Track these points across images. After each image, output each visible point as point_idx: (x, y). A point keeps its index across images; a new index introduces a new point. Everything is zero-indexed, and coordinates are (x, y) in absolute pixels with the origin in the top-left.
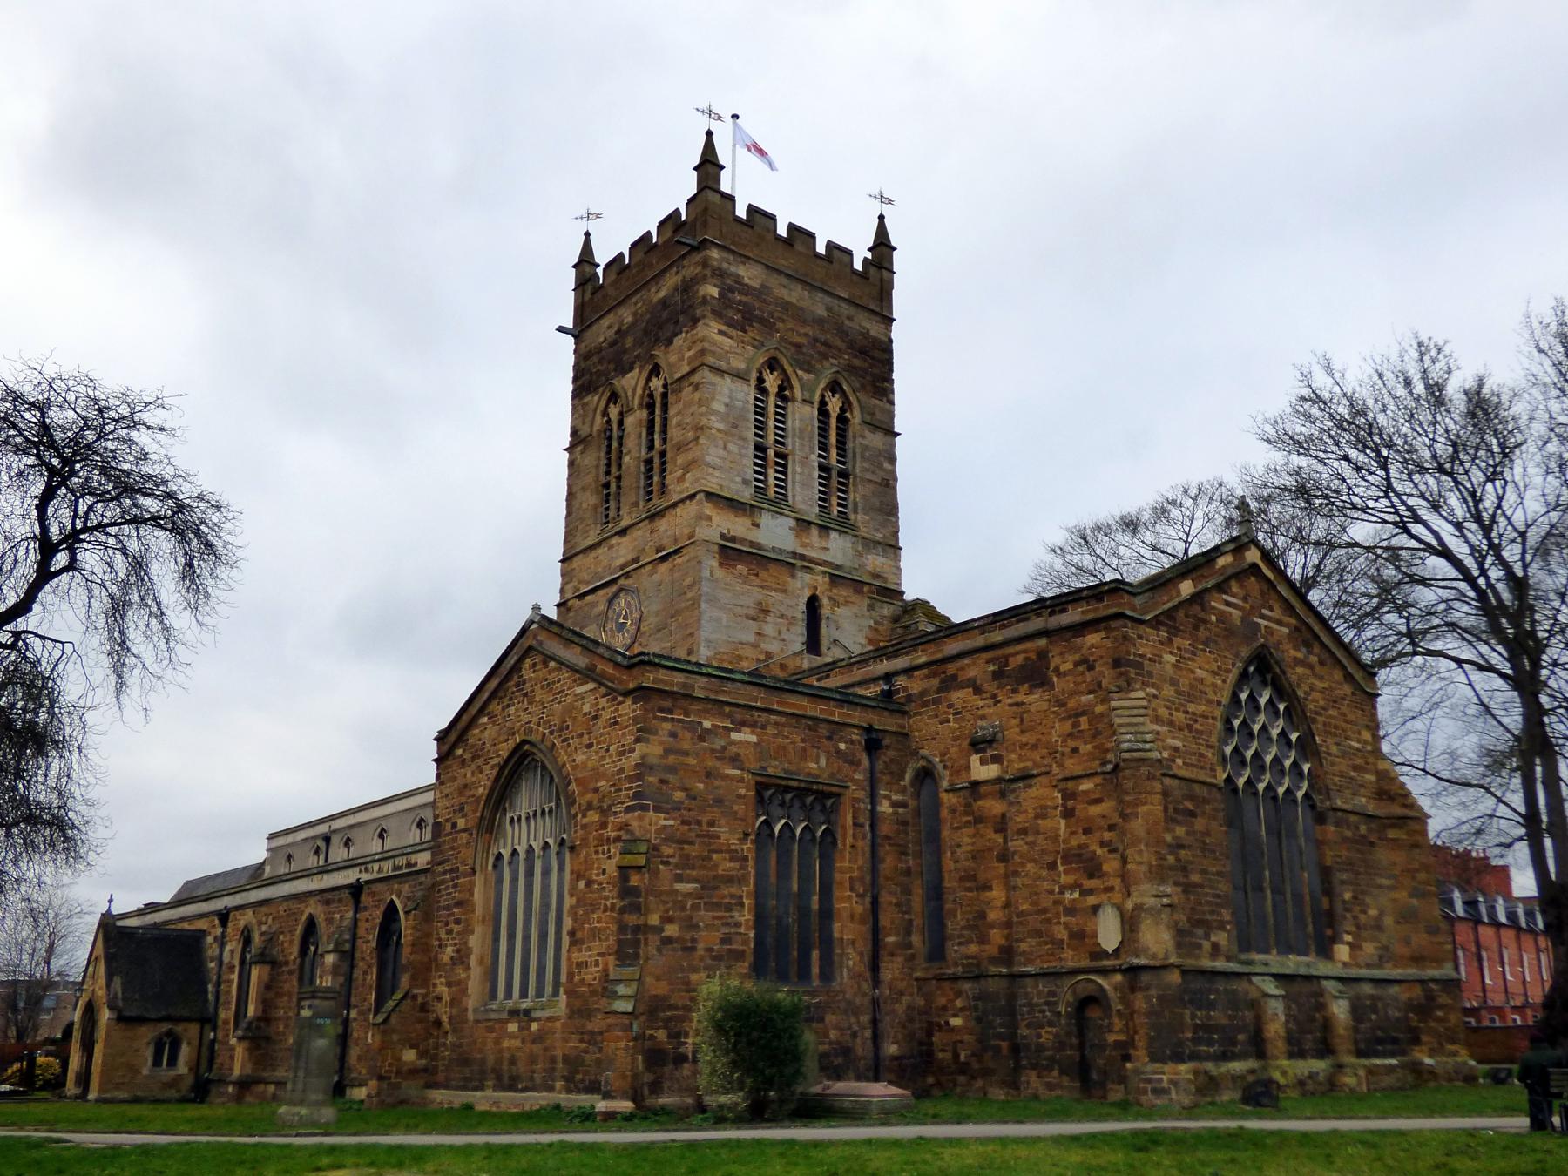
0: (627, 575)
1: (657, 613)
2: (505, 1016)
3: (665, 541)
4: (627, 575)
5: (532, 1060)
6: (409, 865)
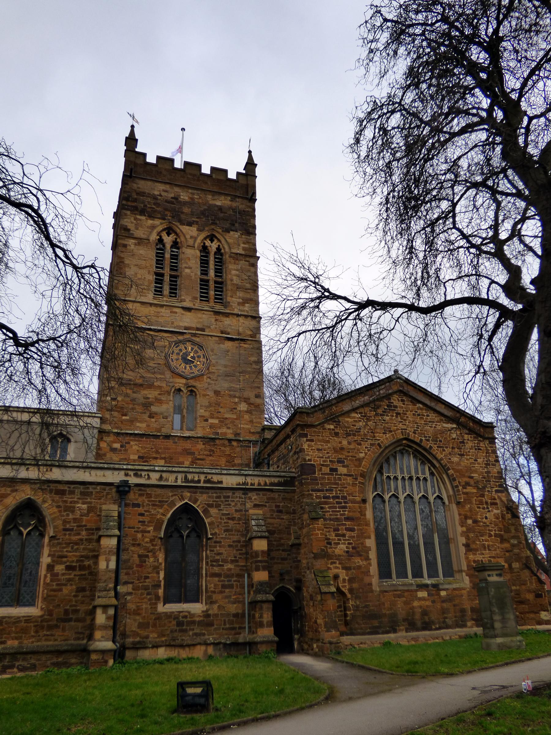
0: (195, 335)
1: (226, 366)
2: (415, 588)
3: (229, 330)
4: (195, 335)
5: (444, 611)
6: (208, 481)
